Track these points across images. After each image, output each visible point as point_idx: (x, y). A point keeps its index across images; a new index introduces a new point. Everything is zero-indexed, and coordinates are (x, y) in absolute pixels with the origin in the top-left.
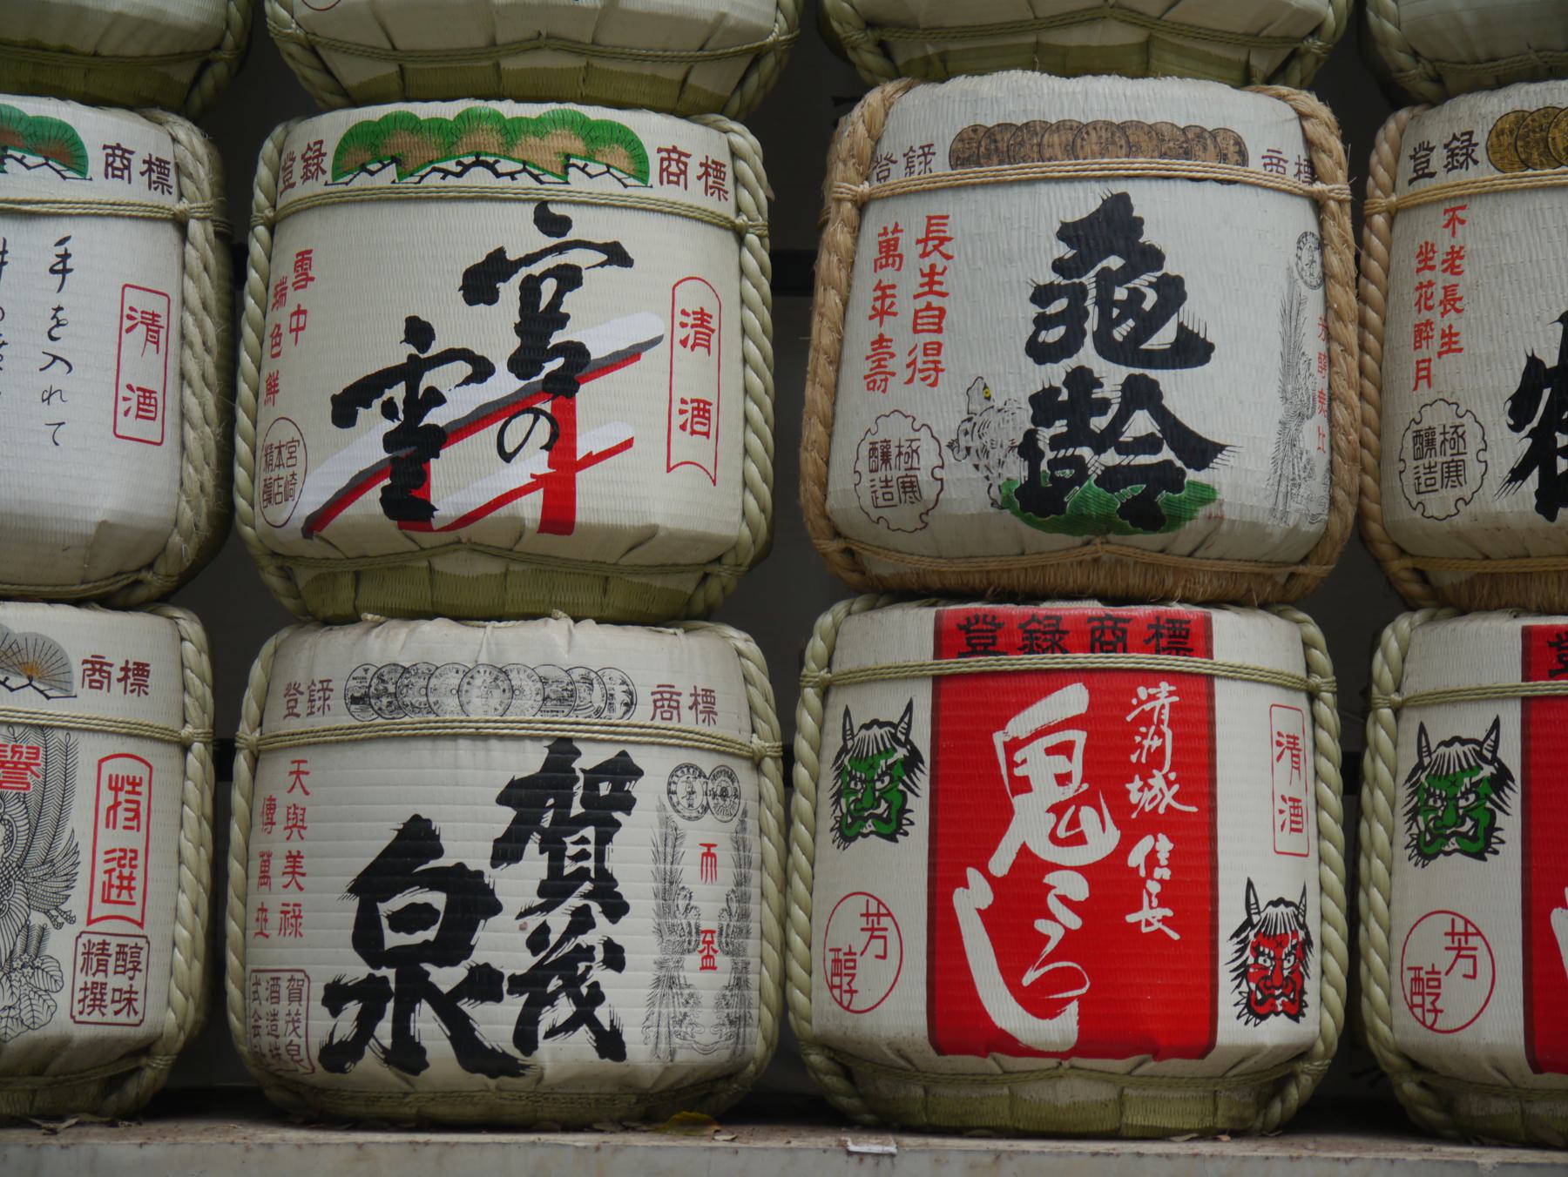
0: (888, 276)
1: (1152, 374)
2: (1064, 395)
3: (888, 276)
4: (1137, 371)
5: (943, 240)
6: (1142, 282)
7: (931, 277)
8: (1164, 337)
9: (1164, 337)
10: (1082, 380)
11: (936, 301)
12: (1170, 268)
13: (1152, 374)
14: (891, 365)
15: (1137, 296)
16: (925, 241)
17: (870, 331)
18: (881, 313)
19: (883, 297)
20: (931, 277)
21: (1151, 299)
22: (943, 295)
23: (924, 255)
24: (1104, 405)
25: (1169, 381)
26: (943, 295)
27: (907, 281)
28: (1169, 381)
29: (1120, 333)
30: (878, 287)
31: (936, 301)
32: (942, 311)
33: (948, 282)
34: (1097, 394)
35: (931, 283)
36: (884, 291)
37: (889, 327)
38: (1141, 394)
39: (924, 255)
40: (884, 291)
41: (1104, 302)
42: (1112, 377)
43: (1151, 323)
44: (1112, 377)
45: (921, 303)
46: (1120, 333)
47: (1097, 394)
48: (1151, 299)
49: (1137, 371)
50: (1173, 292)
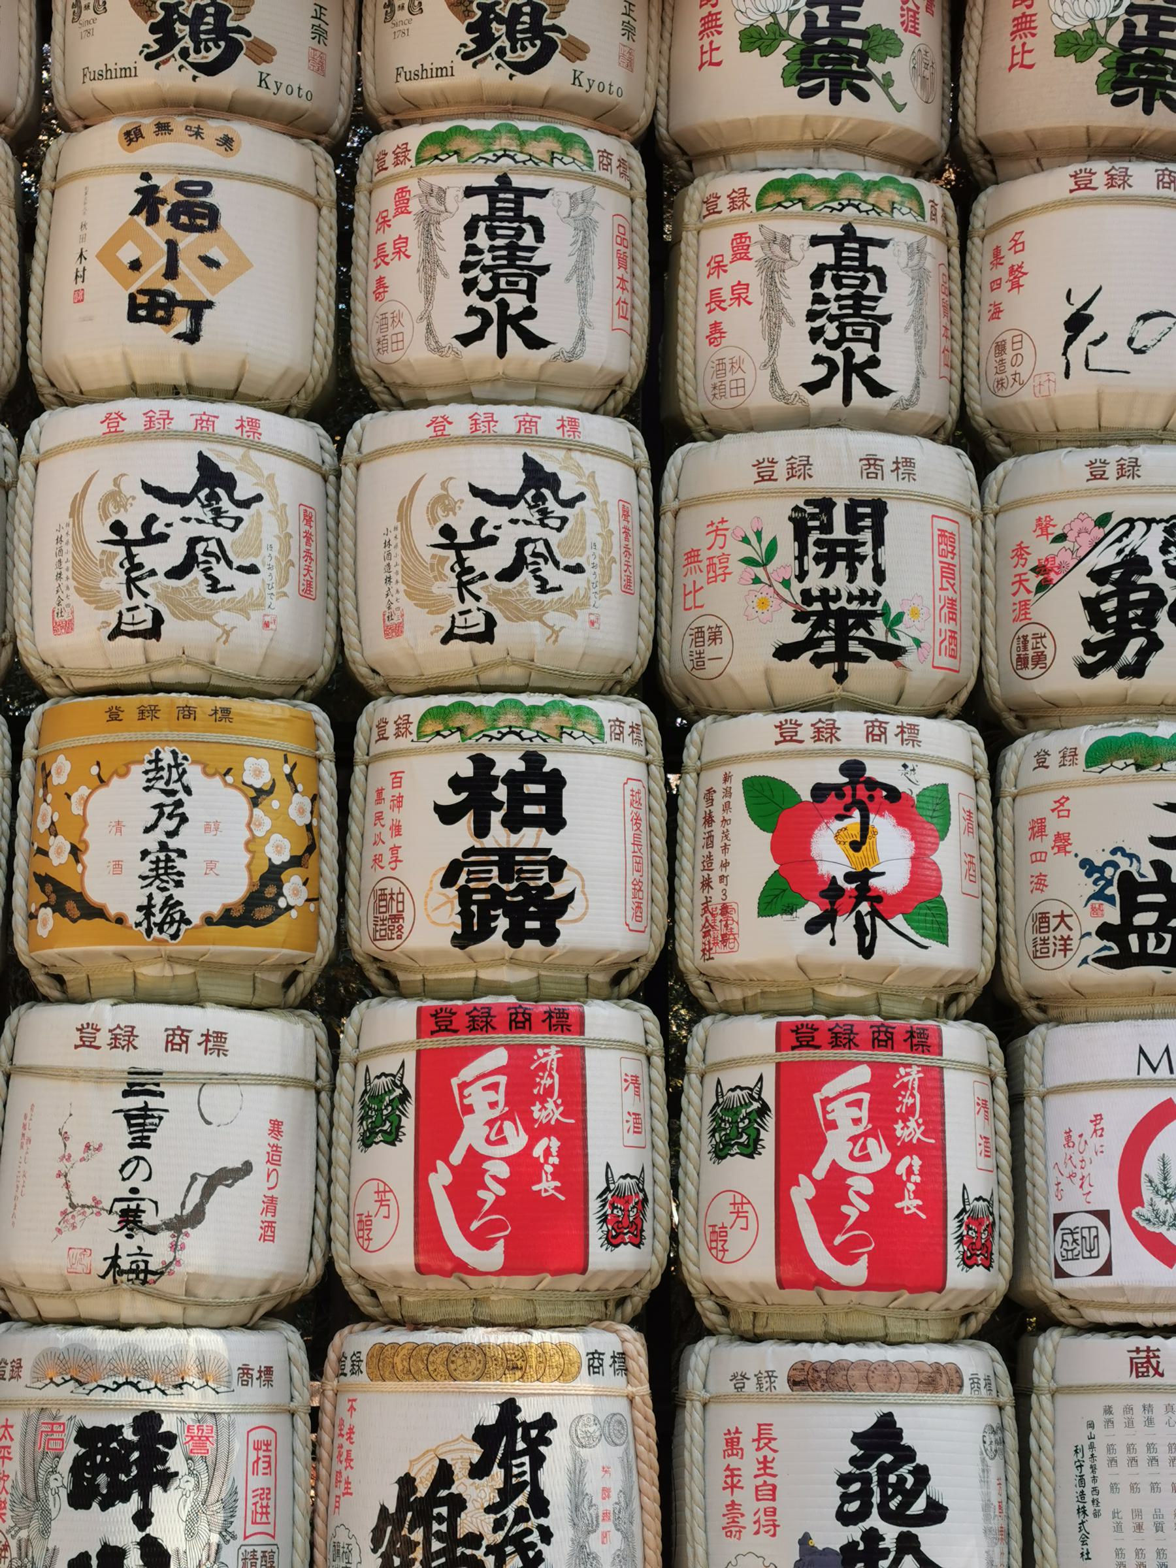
0: (734, 1462)
1: (914, 1530)
2: (861, 1547)
3: (734, 1462)
4: (905, 1529)
5: (770, 1440)
6: (904, 1470)
7: (765, 1464)
8: (919, 1506)
9: (919, 1506)
10: (872, 1536)
11: (770, 1480)
12: (920, 1460)
13: (914, 1530)
14: (742, 1521)
15: (902, 1480)
16: (758, 1440)
17: (727, 1498)
18: (733, 1487)
19: (732, 1476)
20: (765, 1464)
21: (910, 1482)
22: (774, 1476)
23: (758, 1449)
24: (887, 1551)
25: (926, 1536)
26: (774, 1476)
27: (748, 1466)
28: (926, 1536)
29: (893, 1505)
30: (728, 1468)
31: (770, 1480)
32: (774, 1487)
33: (777, 1467)
34: (882, 1545)
35: (765, 1468)
36: (732, 1472)
37: (739, 1496)
38: (908, 1544)
39: (758, 1449)
40: (732, 1472)
41: (883, 1483)
42: (890, 1533)
43: (911, 1497)
44: (890, 1533)
45: (760, 1481)
46: (893, 1505)
47: (882, 1545)
48: (910, 1482)
49: (905, 1529)
50: (922, 1475)
